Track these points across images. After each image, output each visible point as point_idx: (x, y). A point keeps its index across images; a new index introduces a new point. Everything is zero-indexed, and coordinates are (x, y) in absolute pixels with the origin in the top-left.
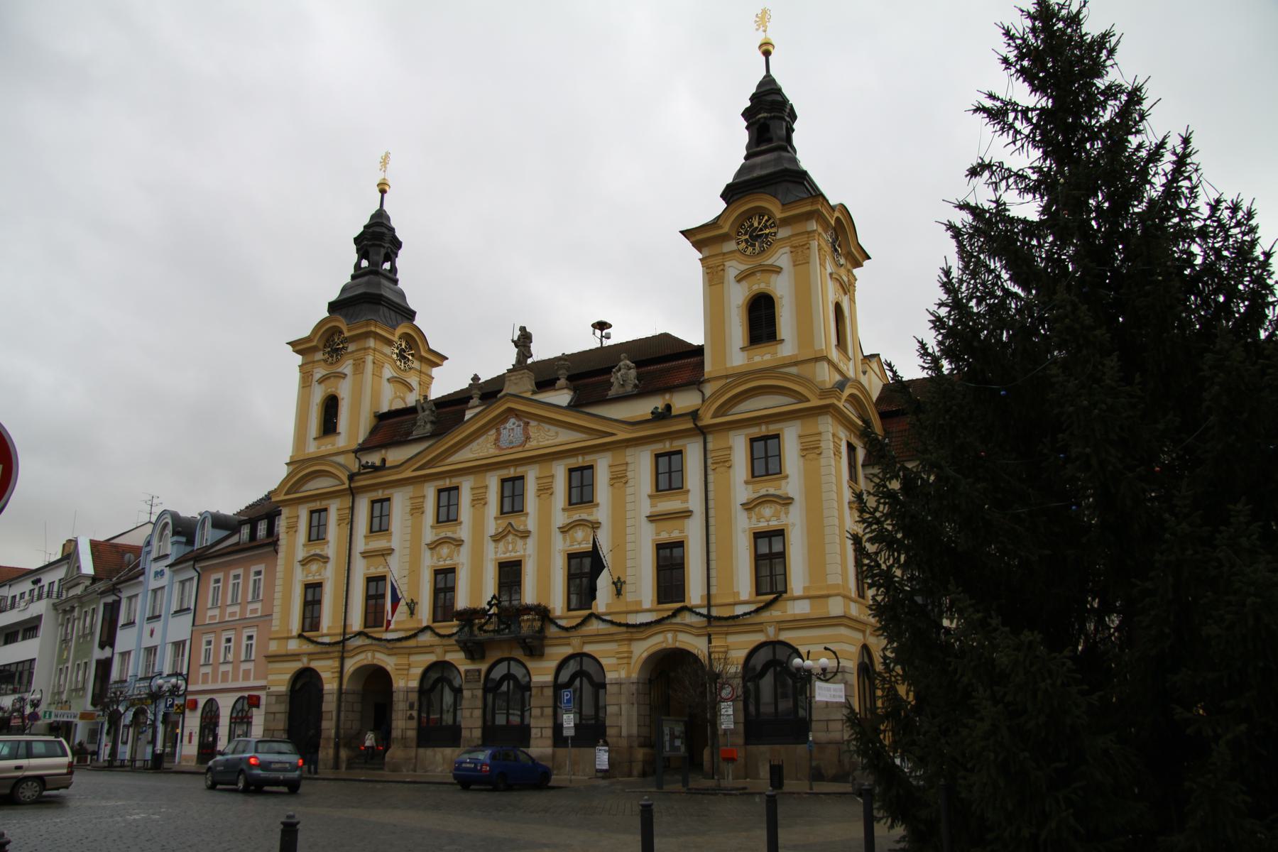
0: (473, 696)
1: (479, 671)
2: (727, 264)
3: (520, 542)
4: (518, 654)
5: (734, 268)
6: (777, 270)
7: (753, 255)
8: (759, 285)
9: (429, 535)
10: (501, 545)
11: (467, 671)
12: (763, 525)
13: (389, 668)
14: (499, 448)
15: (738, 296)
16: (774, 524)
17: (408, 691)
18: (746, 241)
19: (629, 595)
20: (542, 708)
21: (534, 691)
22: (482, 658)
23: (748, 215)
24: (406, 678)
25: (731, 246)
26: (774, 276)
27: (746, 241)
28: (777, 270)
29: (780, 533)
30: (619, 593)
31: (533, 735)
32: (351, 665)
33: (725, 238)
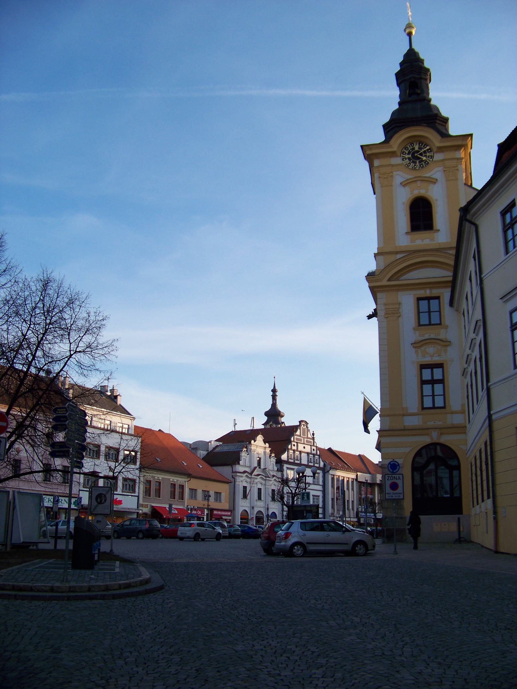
2: (395, 173)
5: (399, 177)
6: (434, 181)
7: (414, 169)
8: (420, 191)
12: (427, 360)
15: (403, 198)
16: (436, 359)
18: (409, 159)
23: (412, 140)
25: (397, 160)
26: (431, 186)
27: (409, 159)
28: (434, 181)
29: (440, 366)
33: (393, 154)
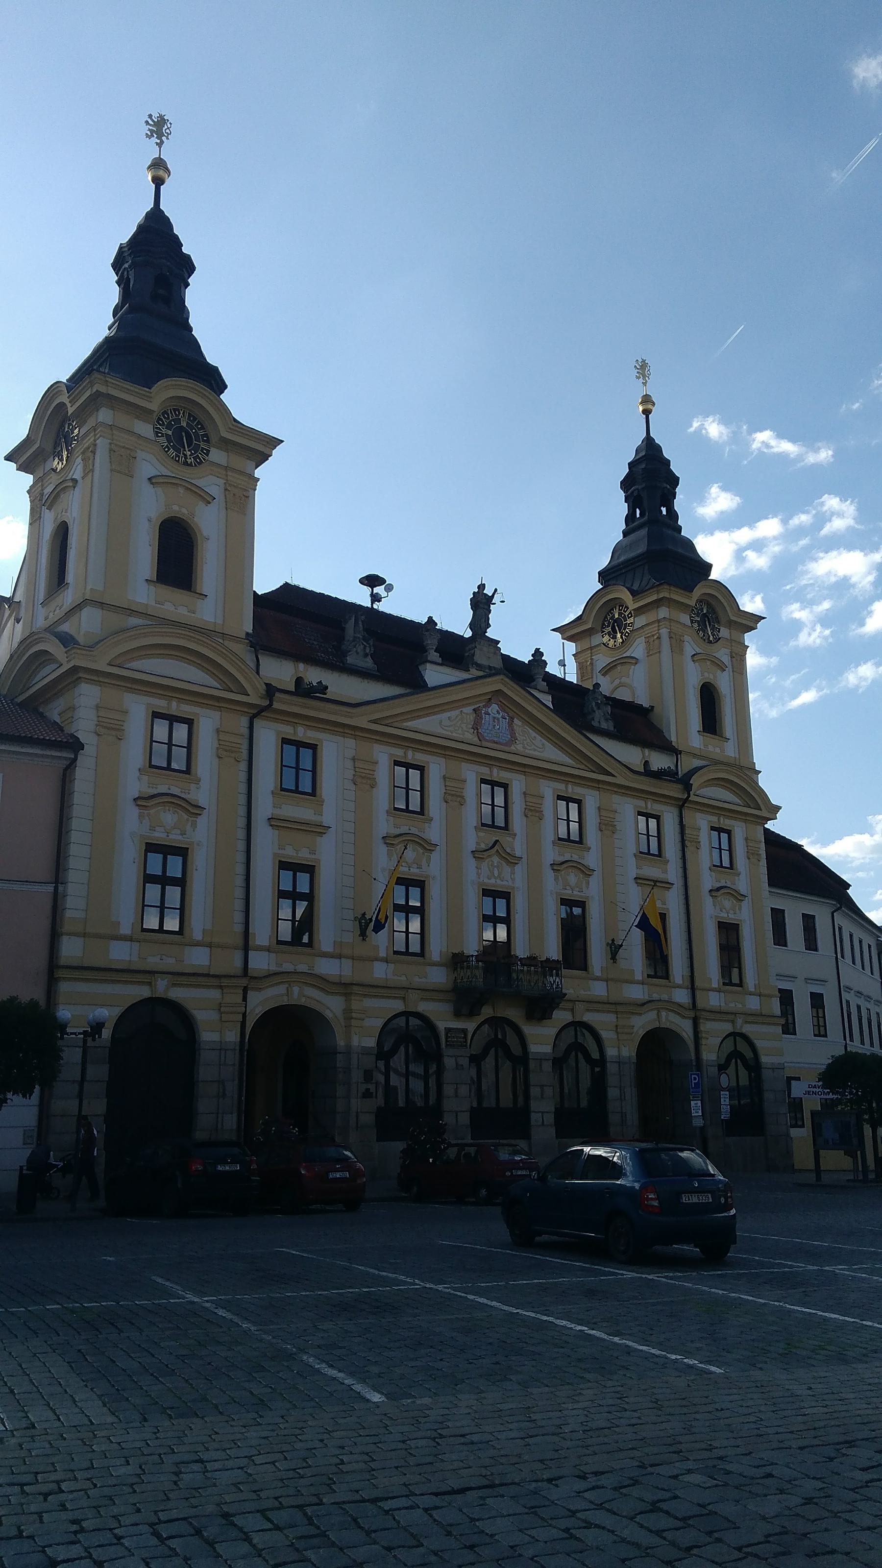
0: (458, 1067)
1: (464, 1031)
3: (507, 869)
4: (514, 1014)
9: (383, 825)
10: (485, 865)
11: (448, 1030)
13: (328, 1014)
14: (480, 737)
17: (366, 1051)
19: (622, 964)
20: (542, 1086)
21: (532, 1065)
22: (472, 1013)
24: (359, 1030)
30: (614, 958)
31: (533, 1122)
32: (260, 1002)
